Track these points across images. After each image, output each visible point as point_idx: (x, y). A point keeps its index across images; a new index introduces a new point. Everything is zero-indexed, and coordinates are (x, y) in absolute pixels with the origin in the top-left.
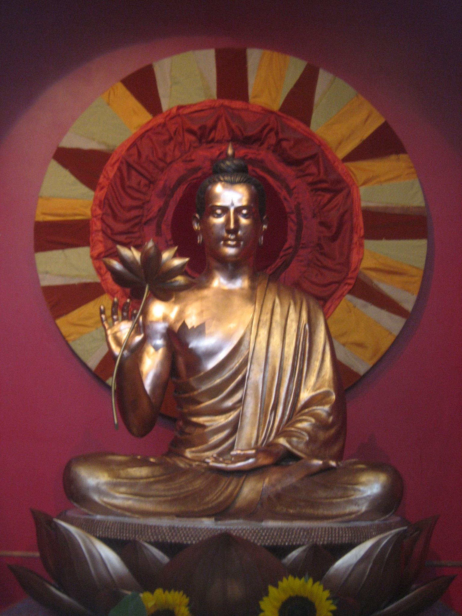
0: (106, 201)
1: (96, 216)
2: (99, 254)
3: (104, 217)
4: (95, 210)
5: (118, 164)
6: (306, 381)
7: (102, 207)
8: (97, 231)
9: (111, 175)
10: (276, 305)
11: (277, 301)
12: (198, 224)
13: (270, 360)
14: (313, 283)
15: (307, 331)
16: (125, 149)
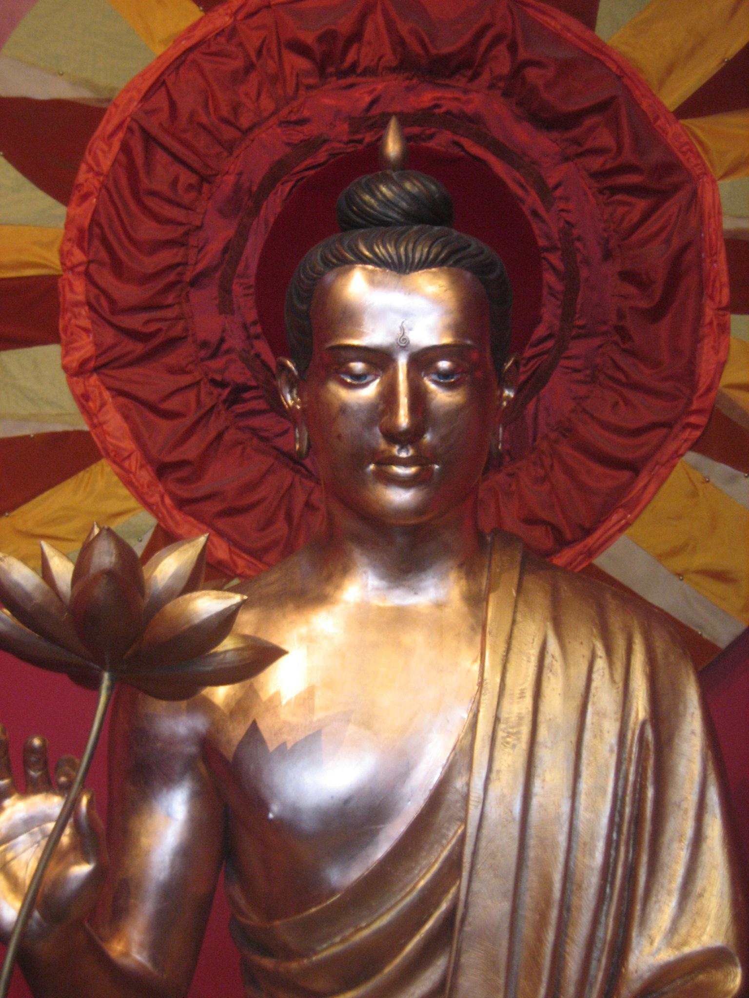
0: (96, 230)
1: (72, 269)
2: (83, 363)
3: (93, 267)
4: (70, 253)
5: (121, 135)
6: (648, 910)
7: (85, 245)
8: (77, 304)
9: (106, 164)
10: (548, 660)
11: (553, 646)
12: (295, 392)
13: (531, 853)
14: (606, 426)
15: (647, 745)
16: (137, 95)
